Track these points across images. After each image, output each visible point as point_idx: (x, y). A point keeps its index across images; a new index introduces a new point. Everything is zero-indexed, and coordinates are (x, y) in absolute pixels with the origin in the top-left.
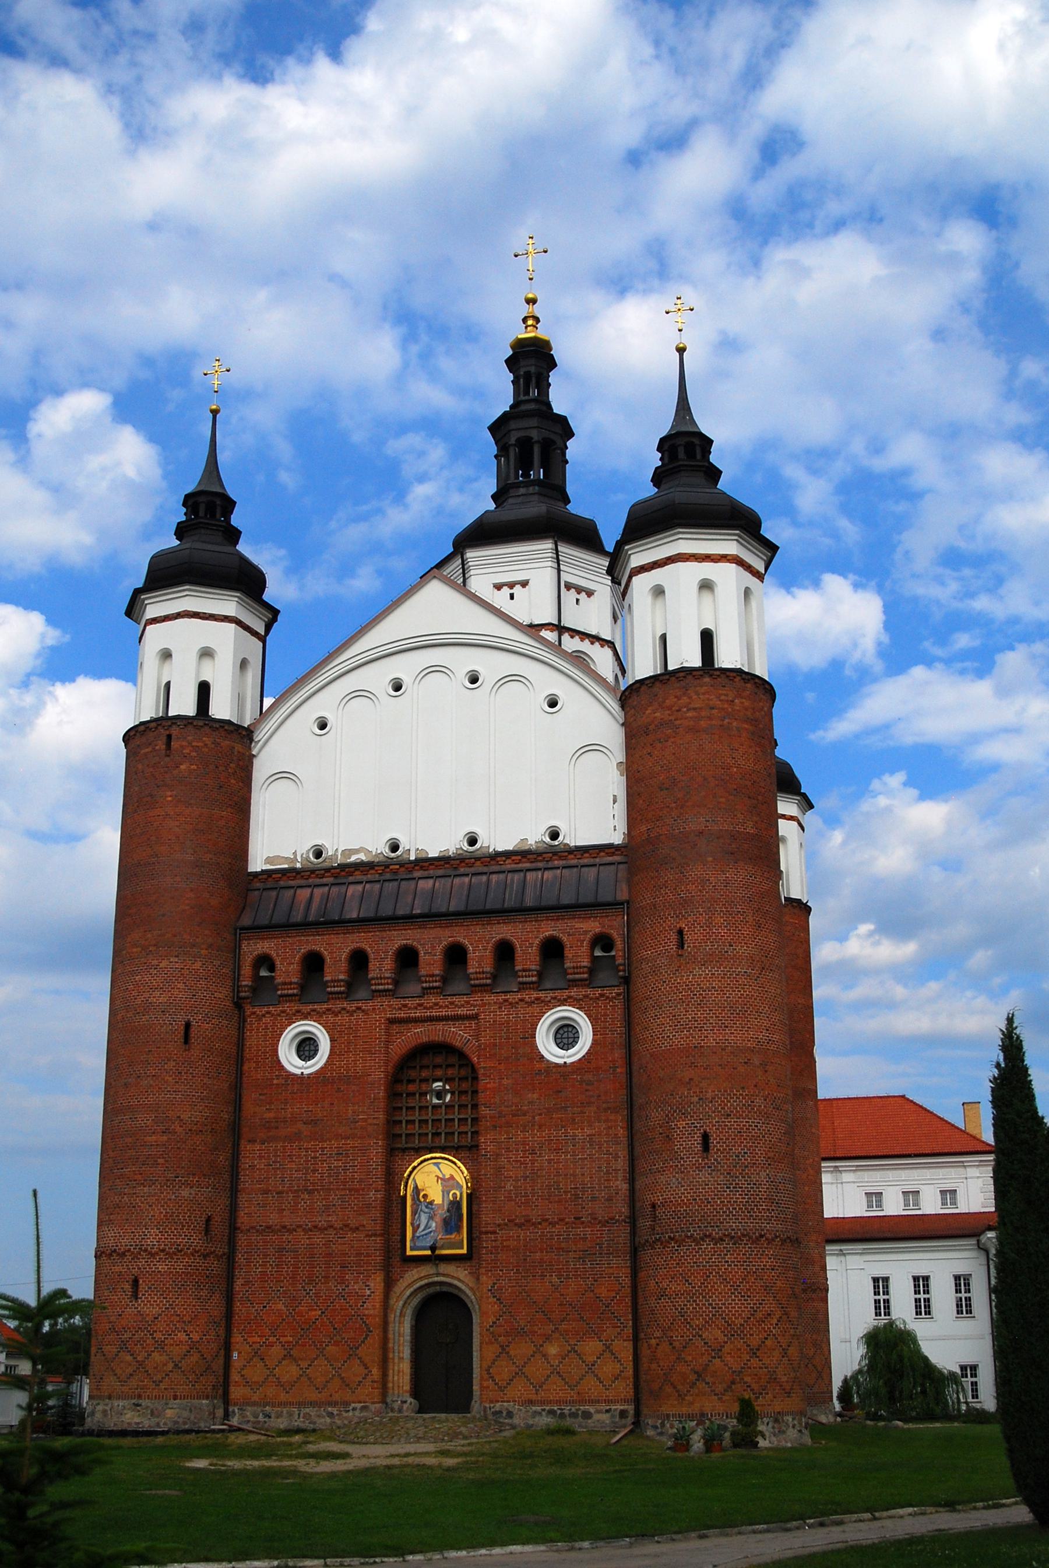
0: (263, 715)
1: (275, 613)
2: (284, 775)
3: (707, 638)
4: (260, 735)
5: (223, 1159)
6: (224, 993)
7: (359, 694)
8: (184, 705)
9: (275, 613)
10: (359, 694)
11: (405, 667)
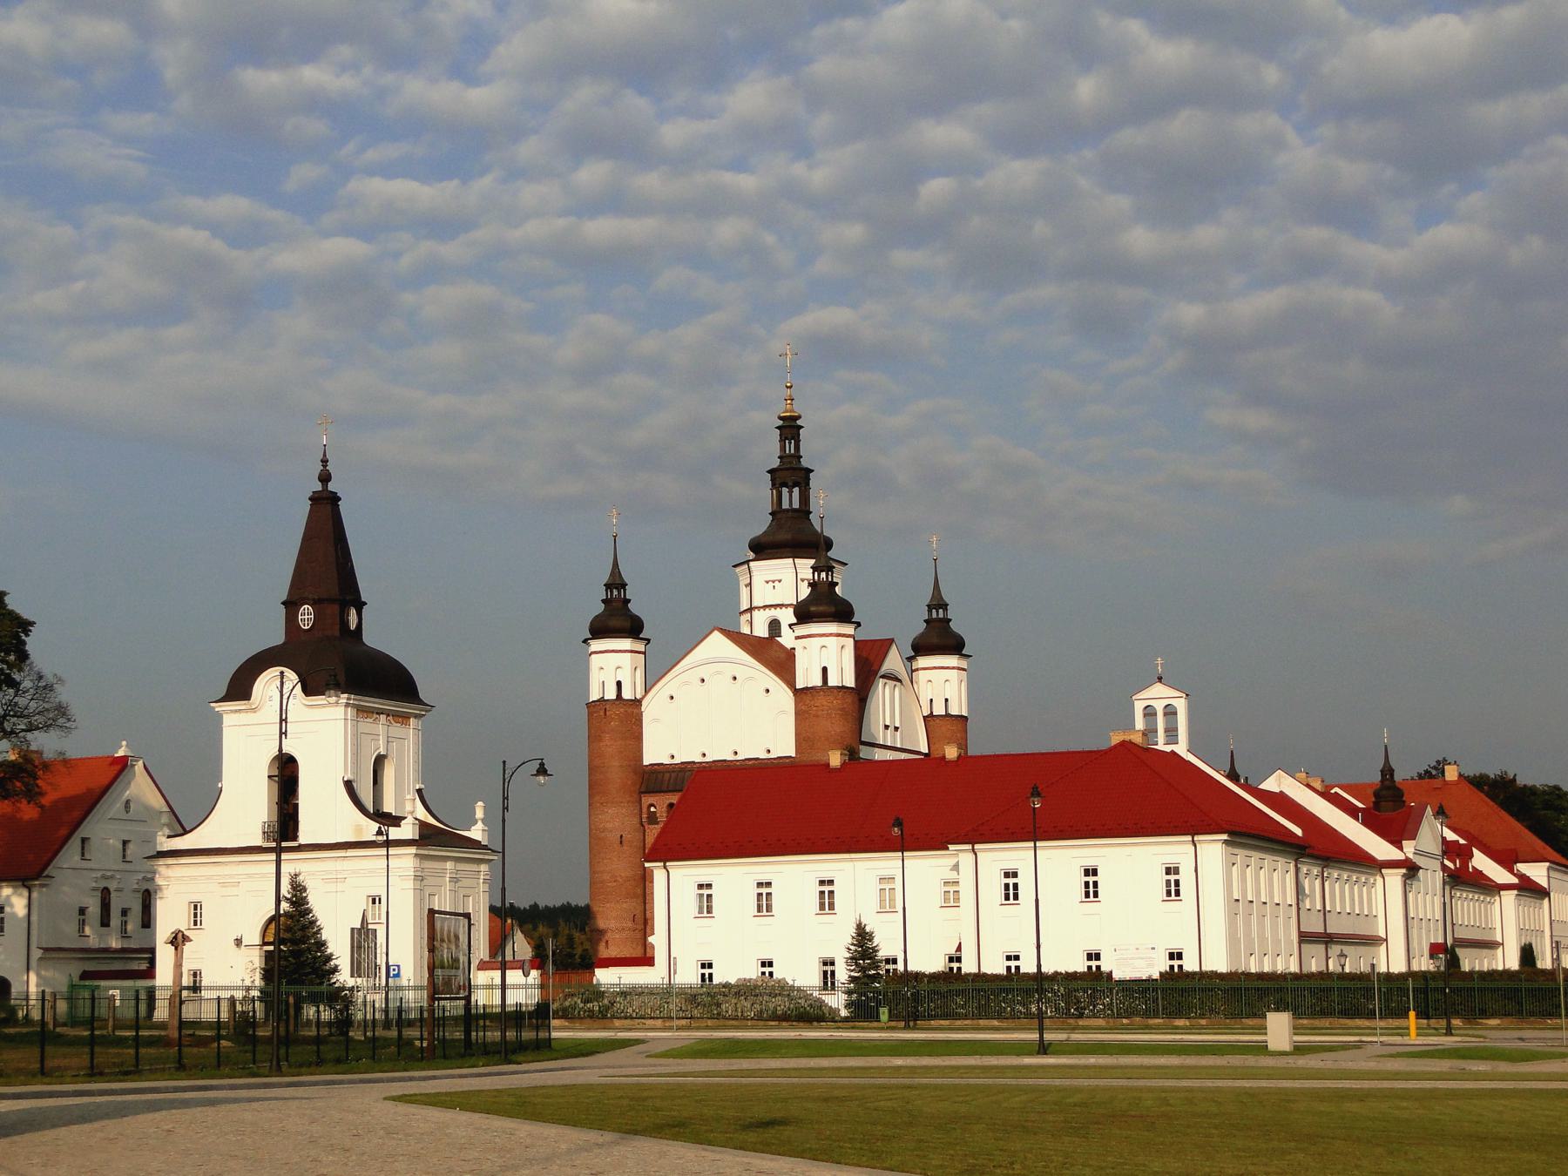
0: (646, 692)
1: (648, 641)
2: (656, 720)
3: (825, 670)
4: (644, 703)
5: (639, 891)
6: (636, 821)
7: (686, 683)
8: (611, 694)
9: (648, 641)
10: (686, 683)
11: (703, 672)
